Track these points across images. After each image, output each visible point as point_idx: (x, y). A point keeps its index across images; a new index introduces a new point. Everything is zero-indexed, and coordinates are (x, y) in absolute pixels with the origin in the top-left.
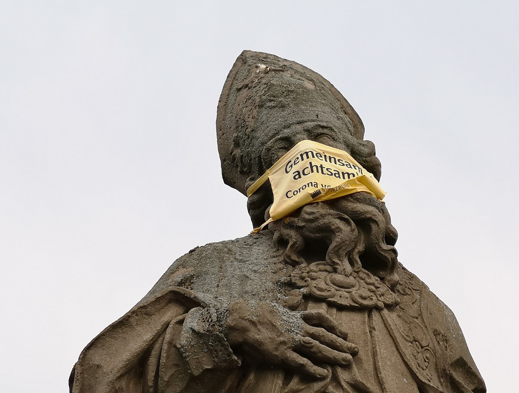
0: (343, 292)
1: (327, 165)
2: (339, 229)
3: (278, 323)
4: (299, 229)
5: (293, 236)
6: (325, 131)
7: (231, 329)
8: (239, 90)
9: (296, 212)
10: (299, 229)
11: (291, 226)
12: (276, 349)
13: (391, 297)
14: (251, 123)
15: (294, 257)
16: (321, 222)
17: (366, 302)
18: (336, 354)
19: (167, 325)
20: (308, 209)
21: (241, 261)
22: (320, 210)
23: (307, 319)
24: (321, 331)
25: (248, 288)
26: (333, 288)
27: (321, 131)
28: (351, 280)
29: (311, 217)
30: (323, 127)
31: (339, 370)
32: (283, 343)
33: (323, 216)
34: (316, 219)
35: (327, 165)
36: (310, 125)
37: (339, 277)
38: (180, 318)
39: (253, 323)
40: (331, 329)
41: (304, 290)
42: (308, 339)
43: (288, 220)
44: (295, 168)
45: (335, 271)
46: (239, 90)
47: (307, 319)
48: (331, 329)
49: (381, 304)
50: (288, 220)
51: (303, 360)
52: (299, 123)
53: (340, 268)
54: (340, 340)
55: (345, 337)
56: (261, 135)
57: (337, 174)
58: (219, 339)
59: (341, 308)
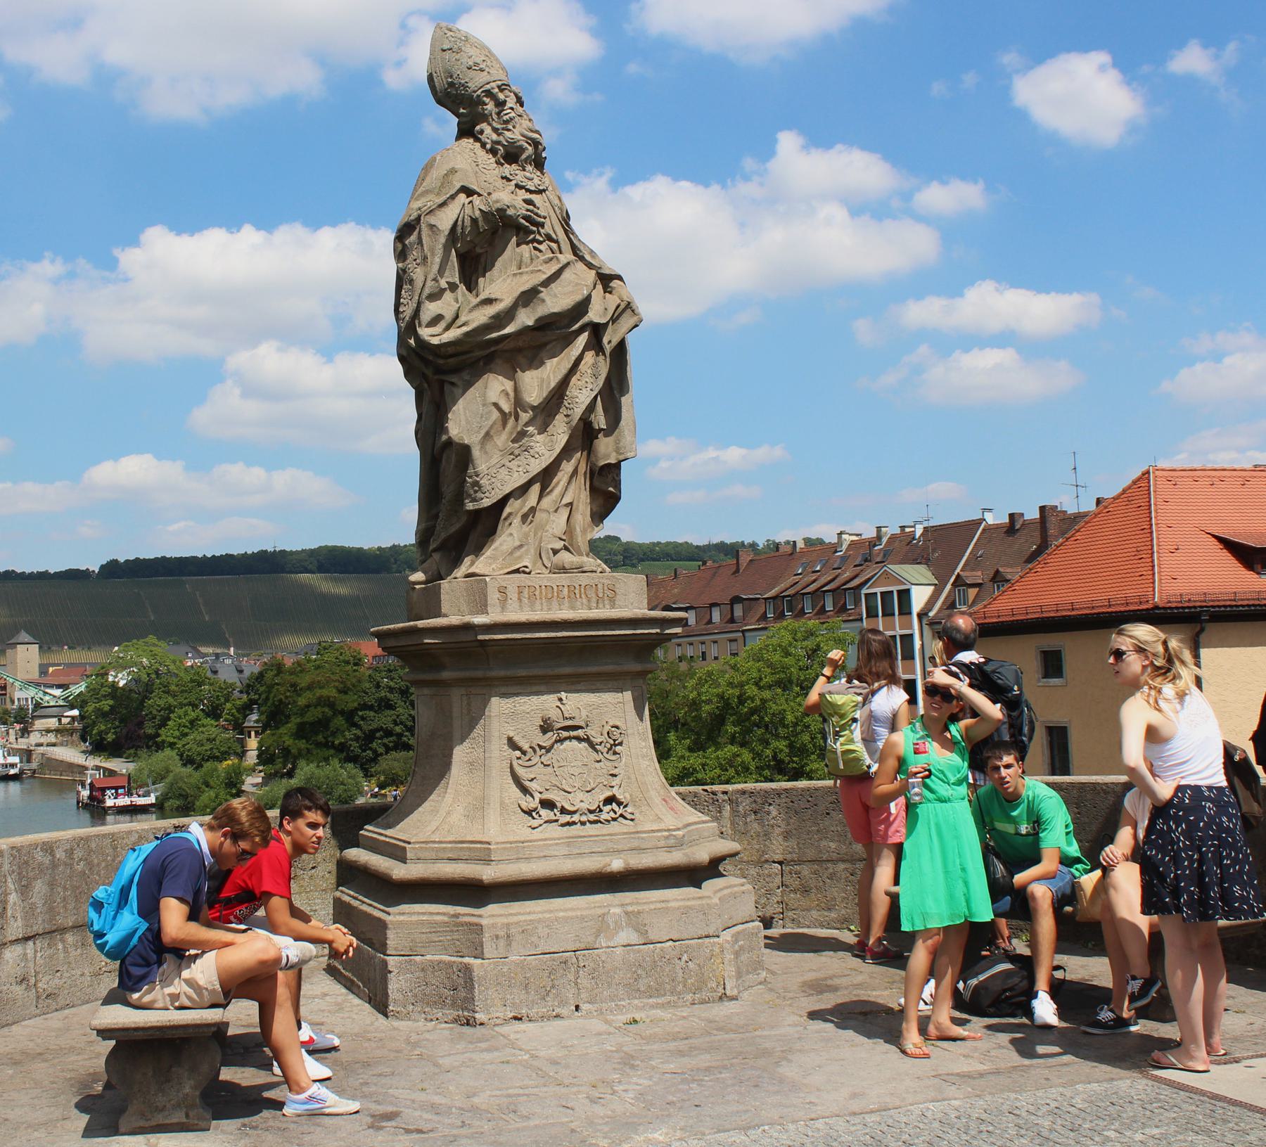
0: (530, 183)
10: (503, 146)
16: (518, 144)
26: (524, 180)
28: (532, 176)
37: (528, 175)
39: (508, 207)
42: (529, 213)
45: (524, 170)
48: (535, 206)
51: (527, 224)
52: (494, 81)
53: (527, 169)
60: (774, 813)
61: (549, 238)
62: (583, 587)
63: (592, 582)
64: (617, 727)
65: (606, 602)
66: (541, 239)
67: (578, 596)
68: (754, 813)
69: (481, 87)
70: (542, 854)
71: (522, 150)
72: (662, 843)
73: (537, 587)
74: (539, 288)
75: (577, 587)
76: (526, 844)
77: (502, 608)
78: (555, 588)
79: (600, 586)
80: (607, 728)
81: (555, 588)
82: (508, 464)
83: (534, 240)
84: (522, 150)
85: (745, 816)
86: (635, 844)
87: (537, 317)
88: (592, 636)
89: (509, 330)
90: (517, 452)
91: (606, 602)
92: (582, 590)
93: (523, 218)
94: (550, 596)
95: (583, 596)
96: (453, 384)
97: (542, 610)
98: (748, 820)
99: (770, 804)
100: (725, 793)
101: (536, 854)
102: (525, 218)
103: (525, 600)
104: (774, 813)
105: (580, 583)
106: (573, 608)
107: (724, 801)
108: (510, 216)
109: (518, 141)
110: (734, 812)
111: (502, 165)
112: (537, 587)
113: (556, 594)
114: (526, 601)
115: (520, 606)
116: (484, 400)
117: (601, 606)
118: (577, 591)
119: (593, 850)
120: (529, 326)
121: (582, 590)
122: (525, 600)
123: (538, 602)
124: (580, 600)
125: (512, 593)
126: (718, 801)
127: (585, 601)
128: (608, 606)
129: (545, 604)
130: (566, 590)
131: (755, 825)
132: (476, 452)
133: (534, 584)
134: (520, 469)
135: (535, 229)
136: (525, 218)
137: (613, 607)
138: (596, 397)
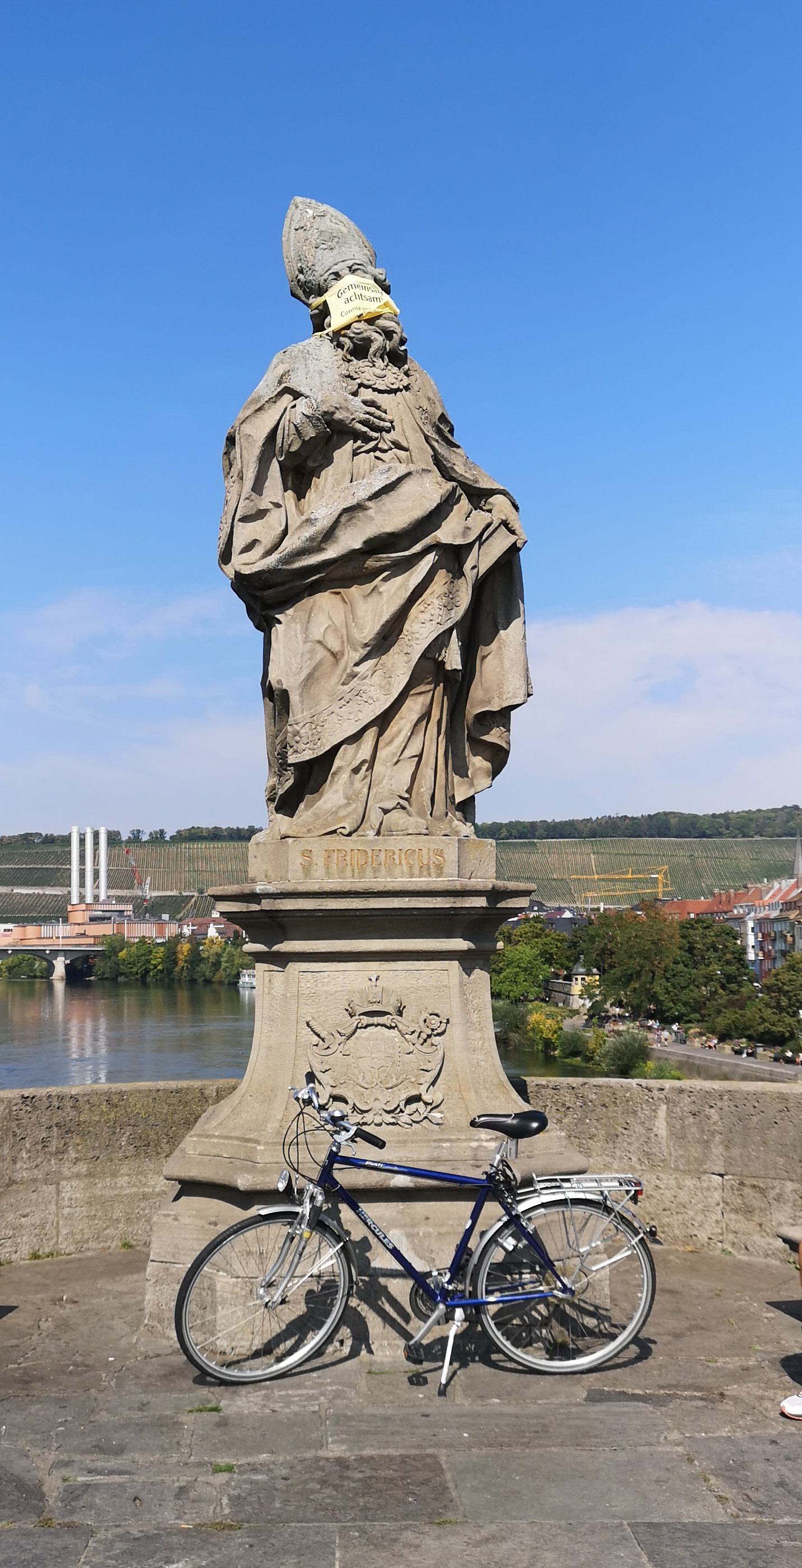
1: (364, 293)
2: (376, 340)
3: (350, 407)
4: (351, 338)
5: (347, 343)
6: (359, 267)
7: (326, 413)
8: (296, 230)
9: (348, 327)
10: (351, 338)
11: (345, 336)
12: (350, 423)
13: (406, 381)
14: (310, 258)
15: (349, 357)
16: (365, 335)
17: (394, 387)
18: (382, 424)
20: (355, 325)
21: (317, 359)
22: (362, 326)
23: (365, 402)
24: (372, 410)
25: (325, 380)
27: (356, 267)
29: (358, 331)
30: (358, 264)
31: (384, 433)
32: (354, 419)
33: (366, 331)
34: (362, 333)
35: (364, 293)
36: (350, 263)
38: (293, 404)
39: (337, 408)
40: (378, 408)
41: (358, 381)
42: (367, 416)
43: (343, 332)
44: (345, 296)
46: (296, 230)
47: (365, 402)
48: (378, 408)
49: (401, 387)
50: (343, 332)
51: (365, 429)
53: (377, 365)
54: (384, 414)
55: (385, 412)
56: (319, 269)
57: (371, 299)
58: (318, 419)
59: (380, 392)
61: (398, 446)
62: (404, 851)
63: (415, 847)
64: (437, 1015)
66: (386, 447)
67: (397, 862)
71: (368, 341)
73: (349, 851)
75: (397, 852)
79: (425, 852)
80: (425, 1015)
82: (337, 710)
83: (375, 449)
84: (368, 341)
87: (364, 539)
89: (331, 553)
91: (433, 870)
92: (403, 857)
93: (360, 422)
95: (404, 862)
96: (280, 622)
102: (364, 423)
108: (341, 421)
111: (349, 361)
112: (349, 851)
114: (335, 867)
116: (307, 637)
118: (396, 857)
120: (355, 550)
125: (319, 860)
127: (405, 868)
128: (433, 875)
130: (383, 855)
132: (294, 698)
133: (343, 848)
134: (352, 717)
135: (375, 435)
136: (364, 423)
138: (450, 631)
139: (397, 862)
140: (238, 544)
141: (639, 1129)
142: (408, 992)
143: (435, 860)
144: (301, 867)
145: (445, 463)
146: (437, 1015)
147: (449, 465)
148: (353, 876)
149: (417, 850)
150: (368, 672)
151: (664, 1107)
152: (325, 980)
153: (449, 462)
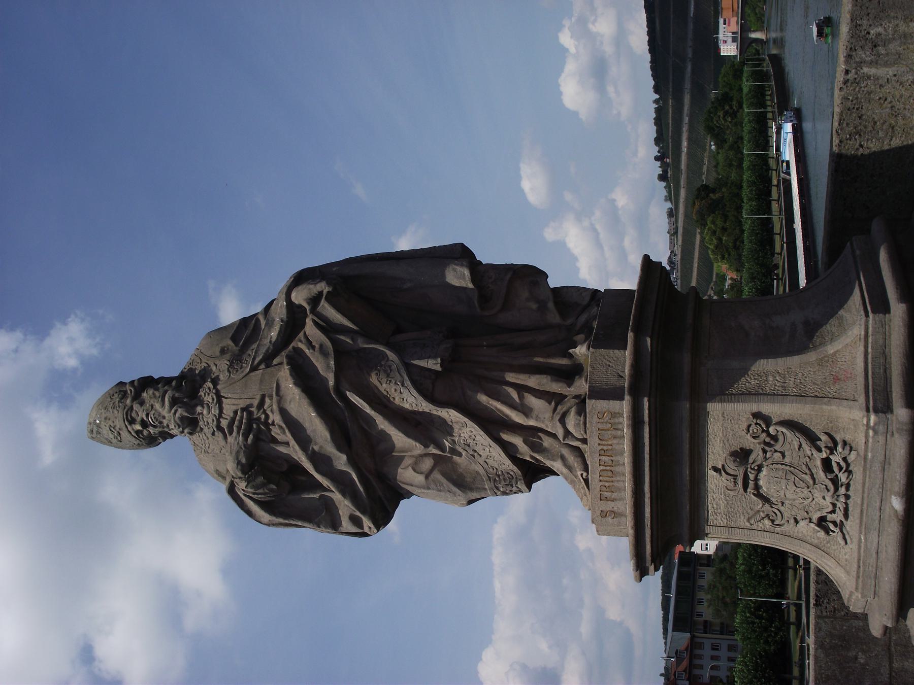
0: (213, 410)
19: (245, 495)
60: (880, 29)
63: (596, 433)
64: (749, 426)
65: (616, 420)
67: (610, 447)
68: (875, 46)
69: (135, 437)
70: (874, 555)
72: (881, 439)
73: (601, 484)
74: (309, 452)
75: (601, 447)
76: (861, 564)
77: (622, 515)
78: (602, 468)
79: (600, 426)
81: (602, 468)
85: (879, 55)
86: (877, 466)
88: (650, 458)
90: (472, 453)
91: (616, 420)
92: (604, 443)
94: (610, 474)
95: (610, 443)
97: (624, 481)
98: (883, 52)
99: (868, 33)
100: (847, 72)
101: (872, 560)
102: (246, 437)
103: (614, 495)
104: (880, 29)
105: (596, 444)
106: (622, 453)
107: (856, 73)
109: (175, 421)
110: (871, 64)
113: (608, 468)
114: (615, 494)
115: (620, 500)
117: (620, 426)
119: (878, 508)
121: (604, 443)
122: (614, 495)
123: (616, 484)
124: (614, 446)
125: (609, 506)
126: (855, 79)
127: (615, 441)
128: (621, 420)
129: (618, 479)
130: (604, 458)
131: (891, 46)
133: (598, 489)
137: (621, 415)
138: (408, 367)
139: (610, 447)
140: (355, 530)
141: (888, 89)
142: (727, 445)
143: (607, 418)
144: (615, 519)
145: (270, 351)
146: (749, 426)
147: (271, 347)
148: (623, 481)
149: (599, 432)
150: (449, 440)
151: (865, 70)
152: (715, 506)
153: (269, 348)
